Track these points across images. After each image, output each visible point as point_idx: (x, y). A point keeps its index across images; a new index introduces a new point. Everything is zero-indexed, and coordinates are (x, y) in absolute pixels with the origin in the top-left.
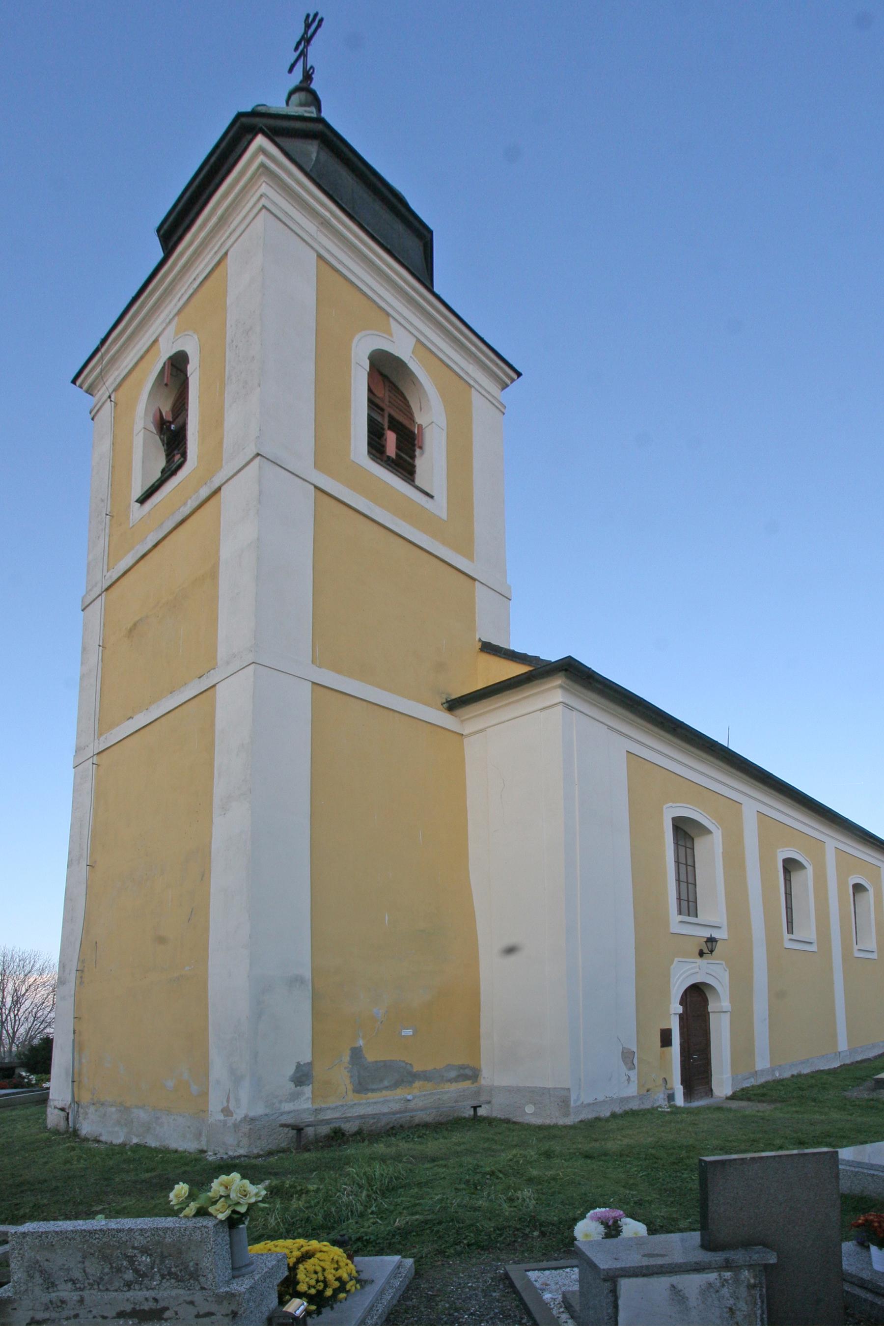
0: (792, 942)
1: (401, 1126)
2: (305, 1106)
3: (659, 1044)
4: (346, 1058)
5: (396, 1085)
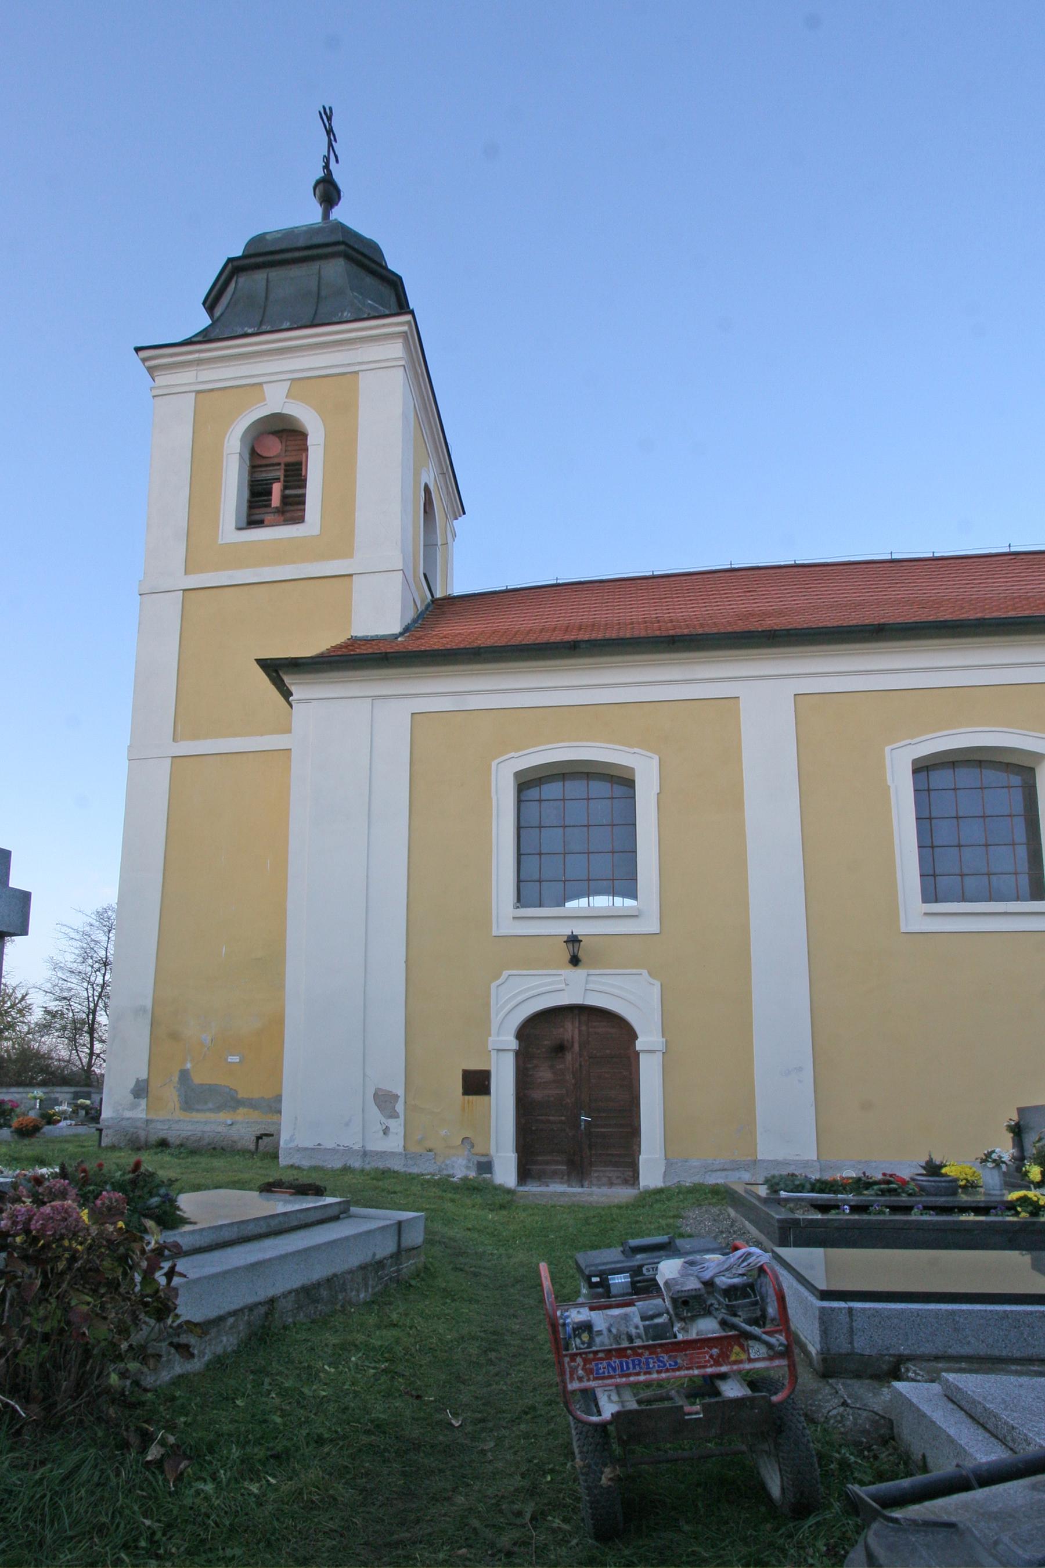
0: (928, 919)
1: (223, 1149)
2: (141, 1116)
3: (460, 1090)
4: (176, 1079)
5: (219, 1109)
